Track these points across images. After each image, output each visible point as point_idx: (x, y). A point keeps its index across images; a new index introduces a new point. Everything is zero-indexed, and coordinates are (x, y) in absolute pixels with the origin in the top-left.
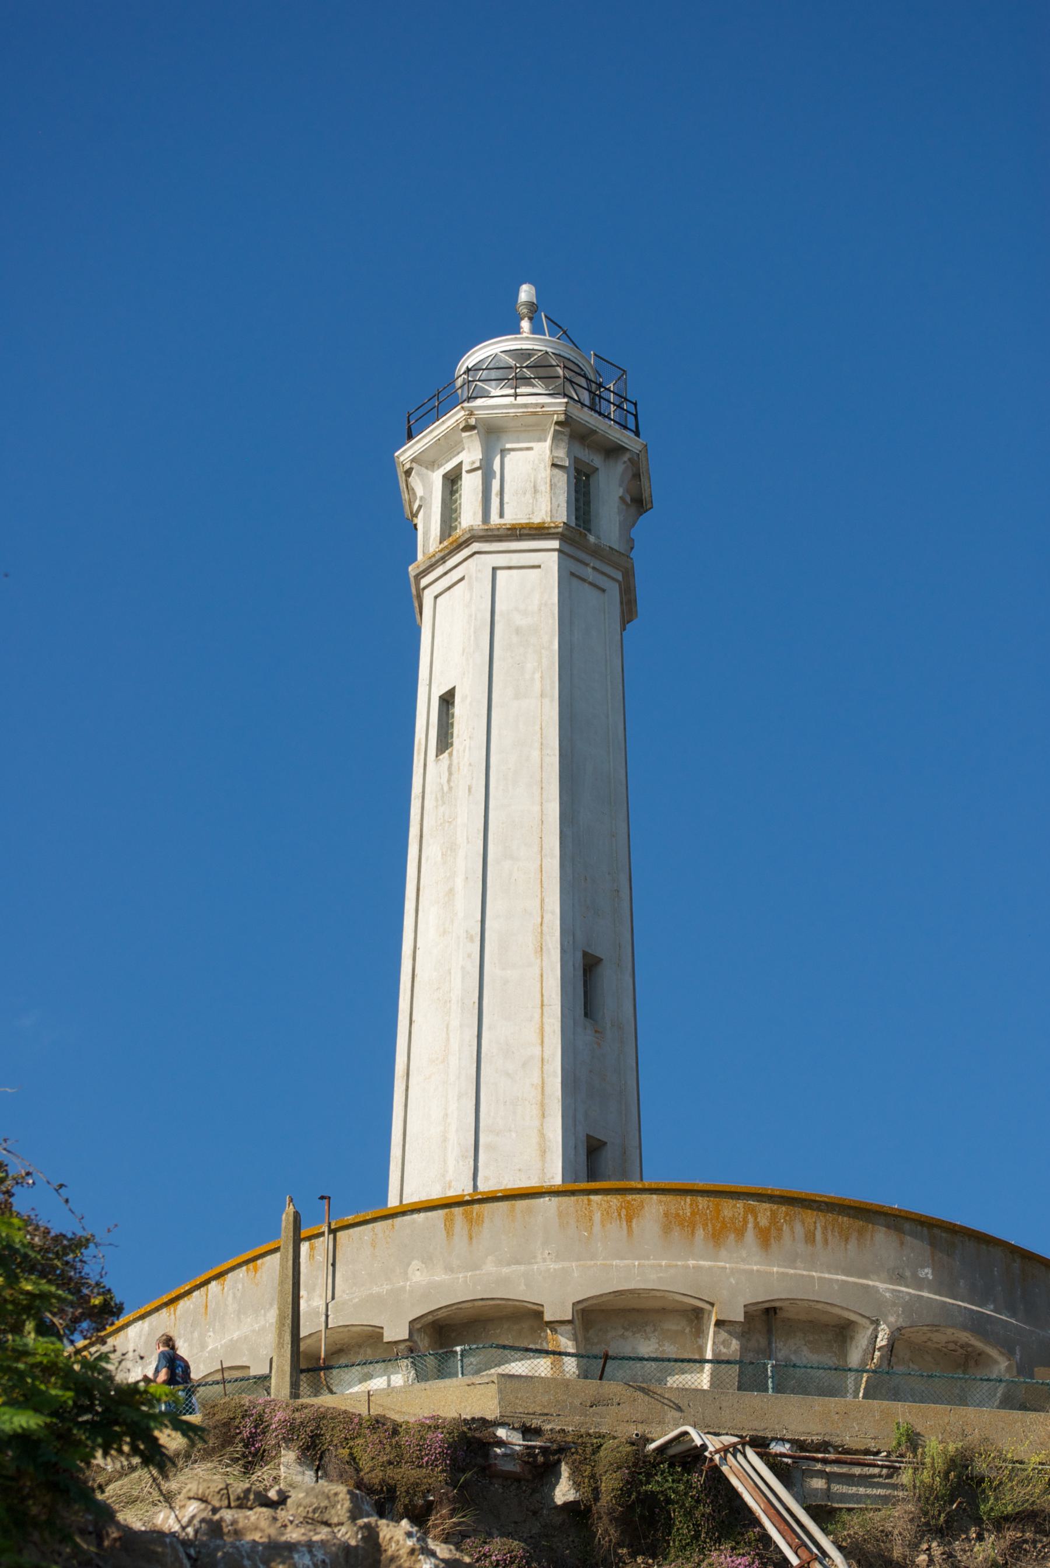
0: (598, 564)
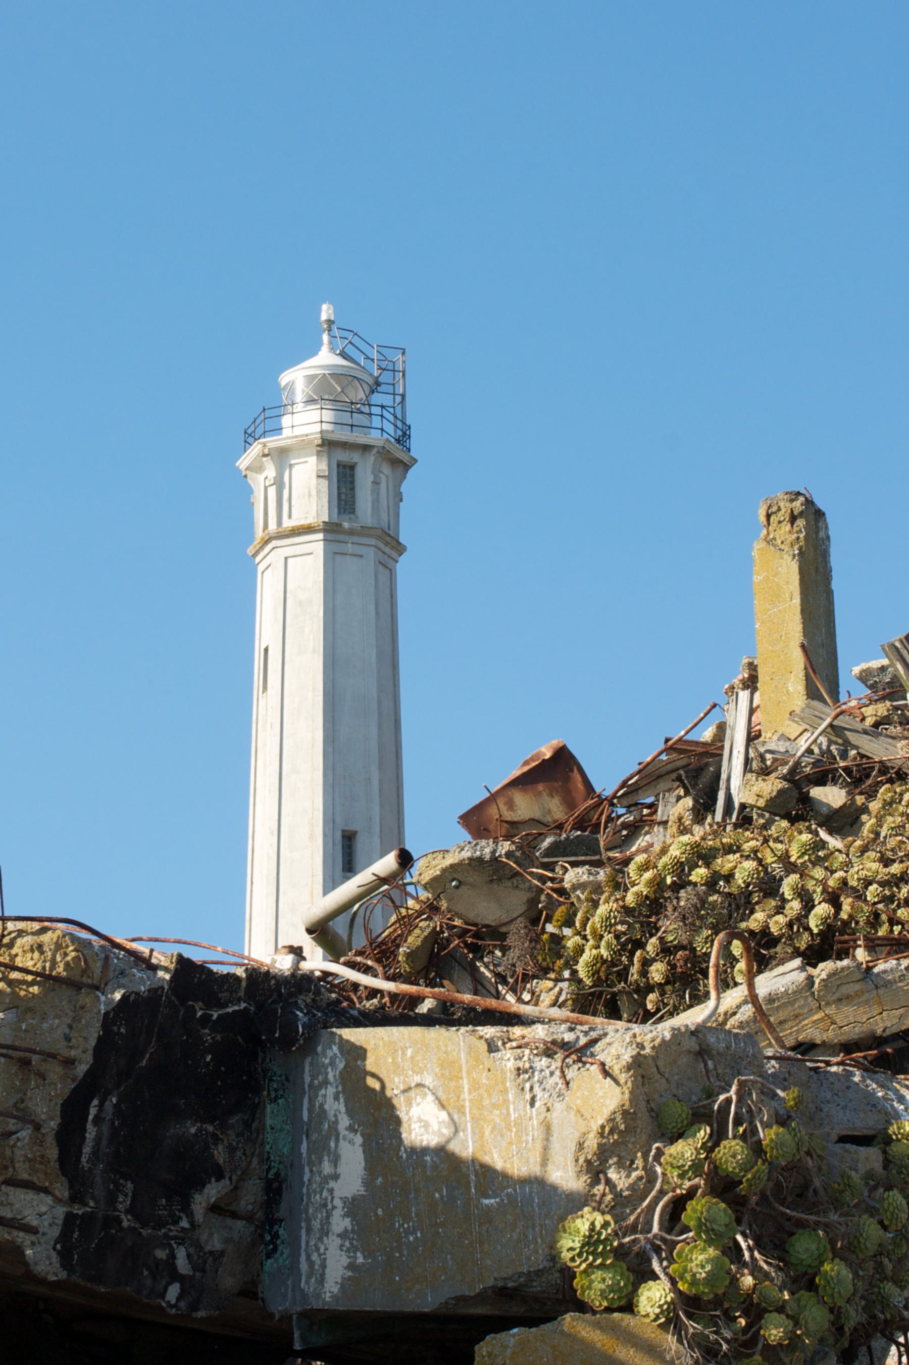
0: (355, 539)
